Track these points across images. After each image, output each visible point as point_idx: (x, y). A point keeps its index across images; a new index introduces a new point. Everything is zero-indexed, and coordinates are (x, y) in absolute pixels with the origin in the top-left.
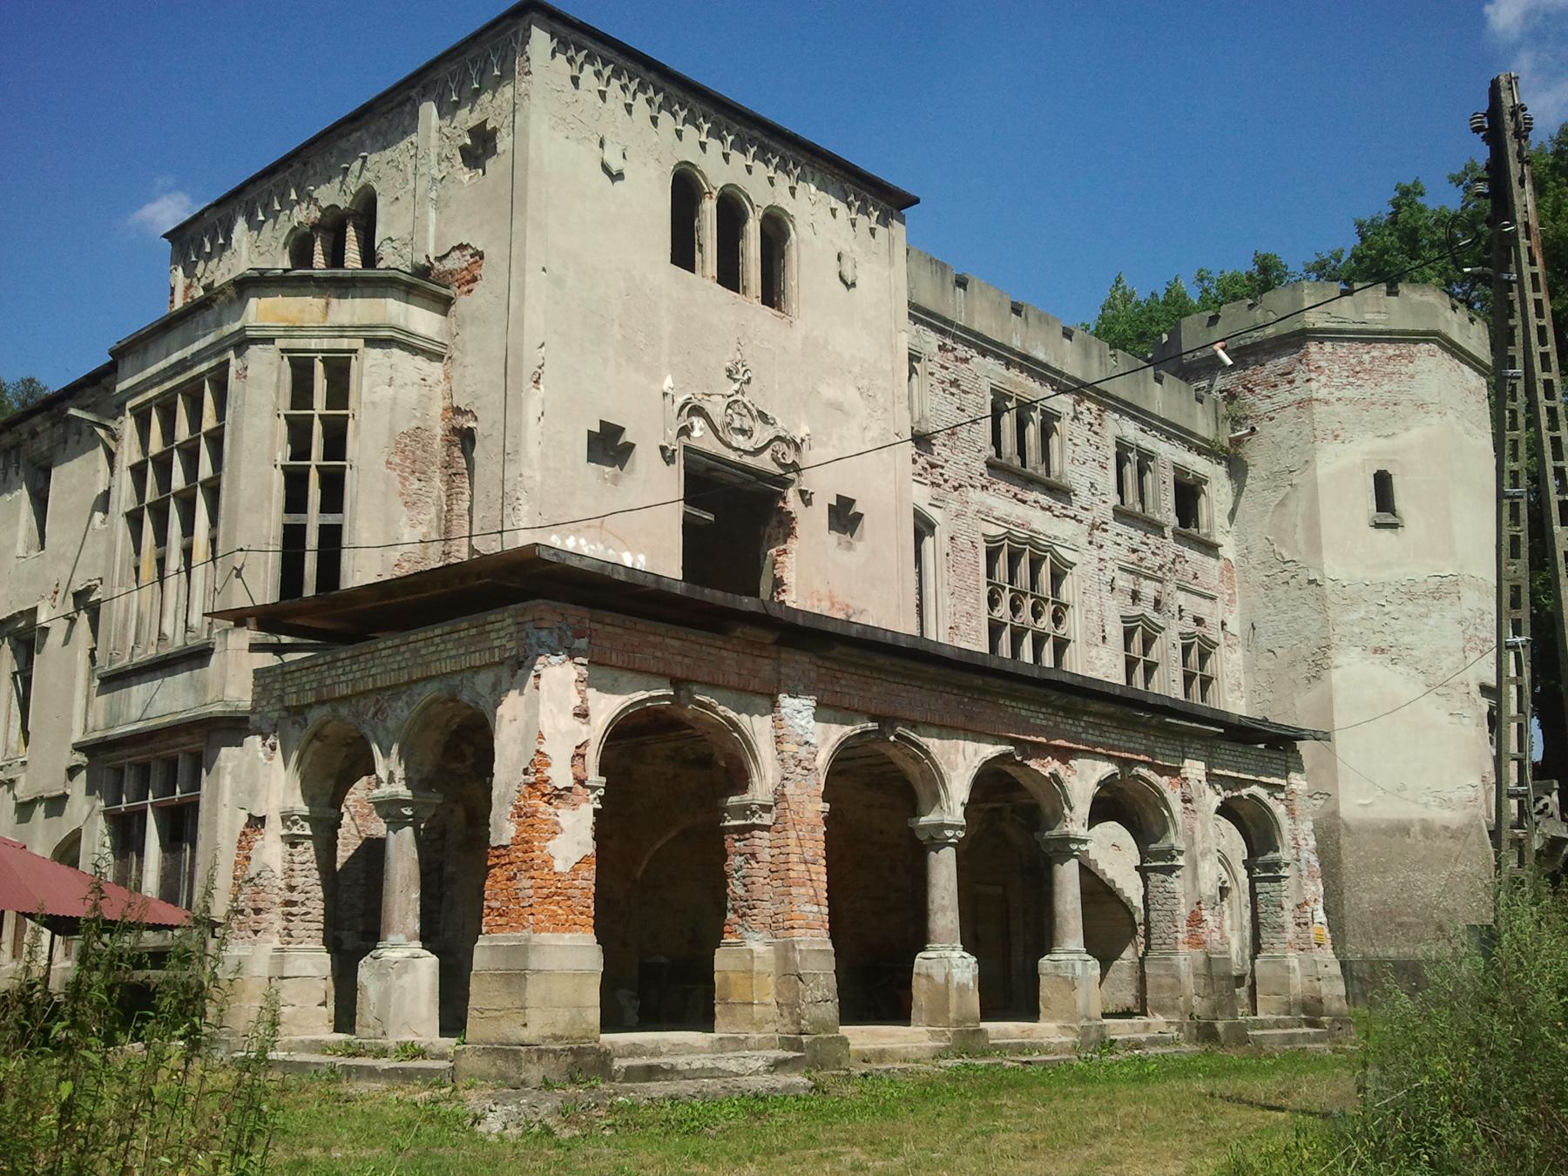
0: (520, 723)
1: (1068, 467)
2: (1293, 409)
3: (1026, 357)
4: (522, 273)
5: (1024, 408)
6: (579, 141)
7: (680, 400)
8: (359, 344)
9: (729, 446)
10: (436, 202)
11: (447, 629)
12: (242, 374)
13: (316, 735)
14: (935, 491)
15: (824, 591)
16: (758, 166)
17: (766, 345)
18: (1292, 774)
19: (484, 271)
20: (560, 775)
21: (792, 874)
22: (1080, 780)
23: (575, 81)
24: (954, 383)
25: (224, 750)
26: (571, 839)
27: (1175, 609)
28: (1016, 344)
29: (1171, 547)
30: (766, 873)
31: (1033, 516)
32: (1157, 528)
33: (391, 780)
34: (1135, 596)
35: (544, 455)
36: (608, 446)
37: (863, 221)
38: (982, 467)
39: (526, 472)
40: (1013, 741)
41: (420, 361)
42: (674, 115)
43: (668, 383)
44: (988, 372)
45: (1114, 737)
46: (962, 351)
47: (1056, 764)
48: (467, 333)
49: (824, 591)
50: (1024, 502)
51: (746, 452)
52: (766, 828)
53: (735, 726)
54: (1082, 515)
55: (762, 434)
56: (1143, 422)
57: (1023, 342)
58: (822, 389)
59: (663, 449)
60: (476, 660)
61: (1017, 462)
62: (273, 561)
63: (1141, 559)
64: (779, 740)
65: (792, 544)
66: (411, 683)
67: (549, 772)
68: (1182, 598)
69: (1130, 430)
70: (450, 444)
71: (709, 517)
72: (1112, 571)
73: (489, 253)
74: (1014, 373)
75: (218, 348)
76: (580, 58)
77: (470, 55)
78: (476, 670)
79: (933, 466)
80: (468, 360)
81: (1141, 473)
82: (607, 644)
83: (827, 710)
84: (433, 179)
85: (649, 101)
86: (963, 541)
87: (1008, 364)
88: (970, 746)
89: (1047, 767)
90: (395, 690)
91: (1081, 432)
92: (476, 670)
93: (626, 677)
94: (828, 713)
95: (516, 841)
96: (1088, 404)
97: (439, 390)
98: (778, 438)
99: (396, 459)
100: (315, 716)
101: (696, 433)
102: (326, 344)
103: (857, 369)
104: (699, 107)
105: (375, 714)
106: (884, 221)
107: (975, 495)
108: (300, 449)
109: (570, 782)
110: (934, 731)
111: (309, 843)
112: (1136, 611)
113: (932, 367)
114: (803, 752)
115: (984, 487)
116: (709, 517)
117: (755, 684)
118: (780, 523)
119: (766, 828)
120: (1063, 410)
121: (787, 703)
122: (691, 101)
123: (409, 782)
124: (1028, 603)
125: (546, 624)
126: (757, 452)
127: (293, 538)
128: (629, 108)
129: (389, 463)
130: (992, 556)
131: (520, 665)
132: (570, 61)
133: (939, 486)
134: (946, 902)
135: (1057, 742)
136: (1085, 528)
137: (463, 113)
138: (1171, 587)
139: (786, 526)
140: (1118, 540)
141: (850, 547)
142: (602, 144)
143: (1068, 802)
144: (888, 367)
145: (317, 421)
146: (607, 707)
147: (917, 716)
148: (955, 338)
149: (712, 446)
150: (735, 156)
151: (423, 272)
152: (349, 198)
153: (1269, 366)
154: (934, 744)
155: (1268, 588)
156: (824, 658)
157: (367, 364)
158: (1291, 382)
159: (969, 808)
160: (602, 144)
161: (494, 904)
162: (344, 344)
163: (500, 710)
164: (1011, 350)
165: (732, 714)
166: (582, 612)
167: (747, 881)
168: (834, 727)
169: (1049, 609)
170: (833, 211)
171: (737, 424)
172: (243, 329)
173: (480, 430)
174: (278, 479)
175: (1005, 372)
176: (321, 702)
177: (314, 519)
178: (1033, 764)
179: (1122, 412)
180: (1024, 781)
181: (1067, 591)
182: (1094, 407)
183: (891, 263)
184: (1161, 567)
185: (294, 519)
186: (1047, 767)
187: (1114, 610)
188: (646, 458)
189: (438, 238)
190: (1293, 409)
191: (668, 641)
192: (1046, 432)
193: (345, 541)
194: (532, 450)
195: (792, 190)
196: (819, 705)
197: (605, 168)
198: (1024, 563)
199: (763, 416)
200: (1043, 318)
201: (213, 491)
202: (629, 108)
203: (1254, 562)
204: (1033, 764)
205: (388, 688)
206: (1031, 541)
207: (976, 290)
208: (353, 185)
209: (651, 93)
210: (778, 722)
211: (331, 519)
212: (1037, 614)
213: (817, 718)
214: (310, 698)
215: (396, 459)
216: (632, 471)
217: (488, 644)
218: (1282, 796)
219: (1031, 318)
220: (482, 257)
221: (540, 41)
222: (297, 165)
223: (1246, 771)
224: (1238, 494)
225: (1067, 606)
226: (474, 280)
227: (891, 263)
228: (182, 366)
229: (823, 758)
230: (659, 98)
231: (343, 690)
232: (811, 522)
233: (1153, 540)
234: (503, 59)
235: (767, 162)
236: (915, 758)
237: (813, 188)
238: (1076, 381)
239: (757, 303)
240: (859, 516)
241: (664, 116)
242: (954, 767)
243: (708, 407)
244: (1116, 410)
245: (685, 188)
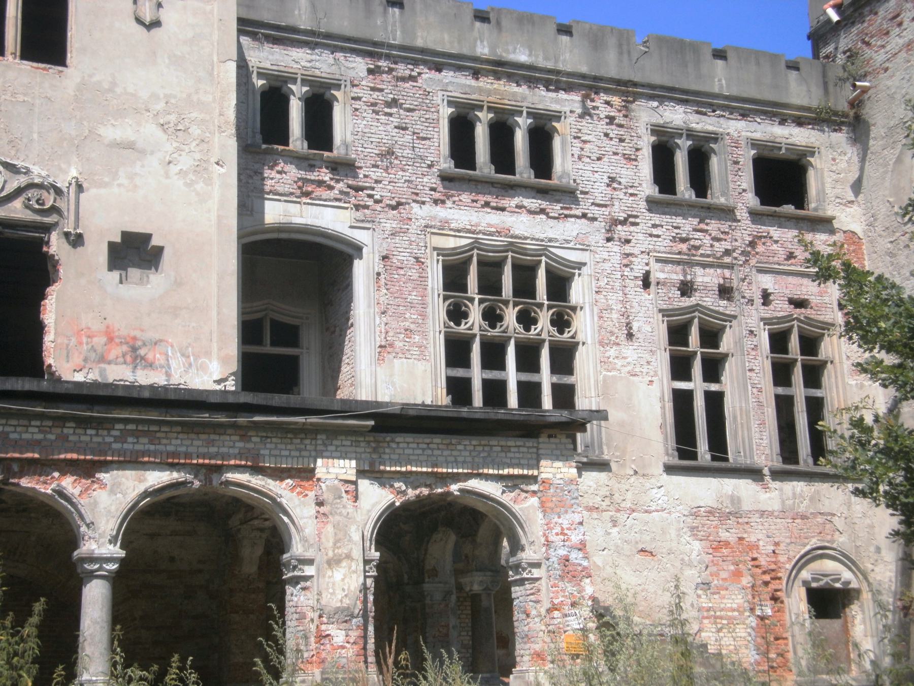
2: (903, 54)
14: (359, 215)
15: (97, 327)
17: (21, 98)
18: (543, 463)
22: (112, 492)
24: (394, 103)
28: (483, 50)
29: (745, 229)
31: (520, 223)
32: (727, 213)
34: (686, 289)
38: (434, 181)
45: (176, 443)
46: (403, 69)
49: (97, 327)
50: (503, 209)
56: (698, 103)
57: (493, 48)
58: (102, 131)
63: (697, 248)
68: (767, 282)
69: (676, 116)
74: (486, 83)
79: (358, 189)
86: (402, 257)
87: (476, 74)
91: (593, 130)
96: (604, 97)
98: (31, 186)
103: (160, 106)
107: (422, 213)
112: (687, 302)
113: (356, 91)
115: (436, 202)
120: (567, 109)
133: (366, 207)
135: (69, 456)
136: (600, 225)
140: (655, 231)
148: (388, 57)
153: (881, 12)
155: (891, 255)
158: (900, 24)
164: (475, 59)
175: (473, 83)
178: (25, 482)
179: (661, 99)
181: (578, 292)
182: (616, 100)
184: (727, 252)
190: (903, 54)
200: (526, 21)
203: (879, 229)
204: (25, 482)
207: (419, 6)
218: (534, 487)
219: (505, 23)
223: (456, 464)
224: (863, 160)
225: (574, 309)
233: (714, 226)
238: (583, 76)
240: (159, 250)
244: (652, 97)
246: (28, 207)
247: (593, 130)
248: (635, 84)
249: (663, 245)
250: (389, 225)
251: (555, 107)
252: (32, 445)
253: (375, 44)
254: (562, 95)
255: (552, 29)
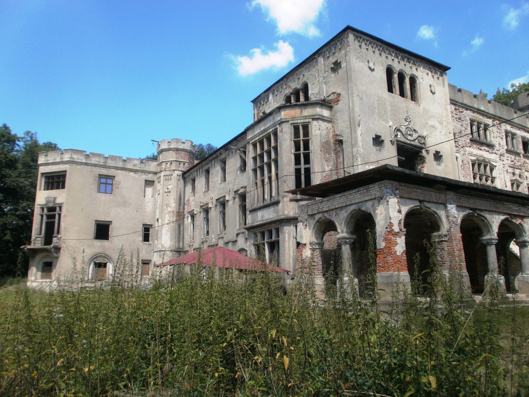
0: (383, 215)
1: (492, 139)
3: (478, 110)
4: (353, 97)
5: (479, 124)
6: (363, 62)
7: (394, 128)
8: (310, 120)
9: (407, 139)
10: (325, 83)
11: (357, 190)
12: (281, 131)
13: (318, 221)
16: (408, 64)
19: (341, 98)
20: (396, 229)
21: (455, 254)
23: (360, 46)
25: (285, 228)
26: (400, 246)
27: (525, 177)
28: (476, 106)
30: (447, 254)
31: (484, 153)
33: (342, 232)
35: (363, 145)
36: (378, 141)
37: (436, 76)
38: (468, 141)
39: (359, 149)
40: (508, 214)
41: (326, 123)
42: (385, 53)
43: (391, 123)
44: (468, 115)
46: (461, 109)
47: (520, 220)
48: (338, 115)
50: (481, 150)
51: (412, 140)
52: (446, 241)
53: (436, 213)
54: (497, 152)
55: (415, 136)
58: (429, 122)
59: (391, 141)
60: (367, 198)
61: (478, 139)
62: (293, 177)
64: (448, 217)
65: (425, 165)
66: (346, 206)
67: (393, 228)
70: (335, 144)
71: (404, 159)
72: (507, 167)
73: (343, 93)
74: (475, 115)
75: (274, 125)
76: (361, 40)
77: (331, 44)
78: (366, 201)
80: (339, 122)
81: (512, 139)
82: (403, 192)
83: (460, 207)
84: (324, 77)
85: (379, 50)
86: (465, 162)
87: (474, 112)
88: (497, 217)
89: (518, 221)
90: (341, 208)
92: (366, 201)
93: (408, 201)
94: (459, 209)
95: (385, 247)
97: (331, 130)
98: (419, 136)
99: (322, 149)
100: (317, 217)
101: (399, 136)
102: (302, 121)
104: (392, 50)
105: (336, 215)
106: (441, 75)
107: (468, 149)
108: (297, 148)
109: (399, 231)
110: (487, 212)
111: (318, 250)
112: (514, 178)
114: (454, 220)
115: (470, 147)
116: (404, 159)
117: (440, 201)
118: (421, 159)
119: (446, 241)
121: (449, 206)
122: (389, 48)
123: (347, 232)
124: (484, 177)
125: (388, 187)
126: (414, 140)
127: (298, 172)
128: (374, 52)
129: (321, 150)
130: (473, 165)
131: (382, 199)
132: (359, 41)
134: (494, 261)
136: (498, 156)
137: (331, 58)
138: (523, 171)
139: (423, 160)
141: (439, 165)
142: (368, 62)
143: (524, 231)
144: (445, 115)
145: (301, 141)
146: (405, 210)
147: (483, 208)
148: (459, 106)
149: (403, 139)
150: (402, 62)
151: (324, 100)
152: (300, 85)
154: (488, 216)
156: (457, 193)
157: (313, 125)
159: (499, 234)
160: (368, 62)
161: (380, 264)
162: (307, 120)
163: (376, 212)
164: (474, 108)
165: (435, 210)
166: (397, 183)
167: (442, 256)
168: (461, 213)
169: (490, 179)
170: (428, 74)
171: (409, 133)
172: (281, 119)
173: (344, 139)
174: (293, 157)
176: (319, 213)
177: (303, 166)
180: (510, 225)
181: (495, 174)
183: (444, 86)
185: (298, 167)
186: (518, 221)
187: (508, 178)
188: (387, 144)
189: (326, 92)
191: (418, 190)
192: (485, 130)
193: (311, 171)
194: (360, 144)
195: (417, 69)
196: (457, 206)
197: (370, 68)
198: (482, 167)
199: (415, 130)
201: (276, 161)
202: (374, 52)
205: (339, 208)
206: (484, 161)
208: (301, 82)
209: (379, 47)
210: (447, 211)
211: (307, 166)
212: (487, 181)
213: (458, 211)
214: (316, 212)
215: (322, 149)
216: (384, 147)
217: (370, 194)
220: (340, 95)
221: (351, 37)
222: (285, 79)
225: (495, 178)
226: (338, 101)
227: (444, 86)
228: (265, 130)
229: (459, 221)
230: (381, 49)
231: (326, 209)
232: (430, 158)
234: (341, 44)
235: (409, 62)
236: (483, 220)
237: (422, 68)
239: (410, 100)
240: (441, 156)
241: (383, 54)
242: (493, 222)
243: (401, 129)
245: (389, 72)
246: (419, 142)
247: (495, 129)
248: (502, 118)
249: (509, 162)
250: (462, 152)
251: (488, 123)
252: (516, 211)
253: (456, 102)
254: (488, 120)
255: (487, 102)
